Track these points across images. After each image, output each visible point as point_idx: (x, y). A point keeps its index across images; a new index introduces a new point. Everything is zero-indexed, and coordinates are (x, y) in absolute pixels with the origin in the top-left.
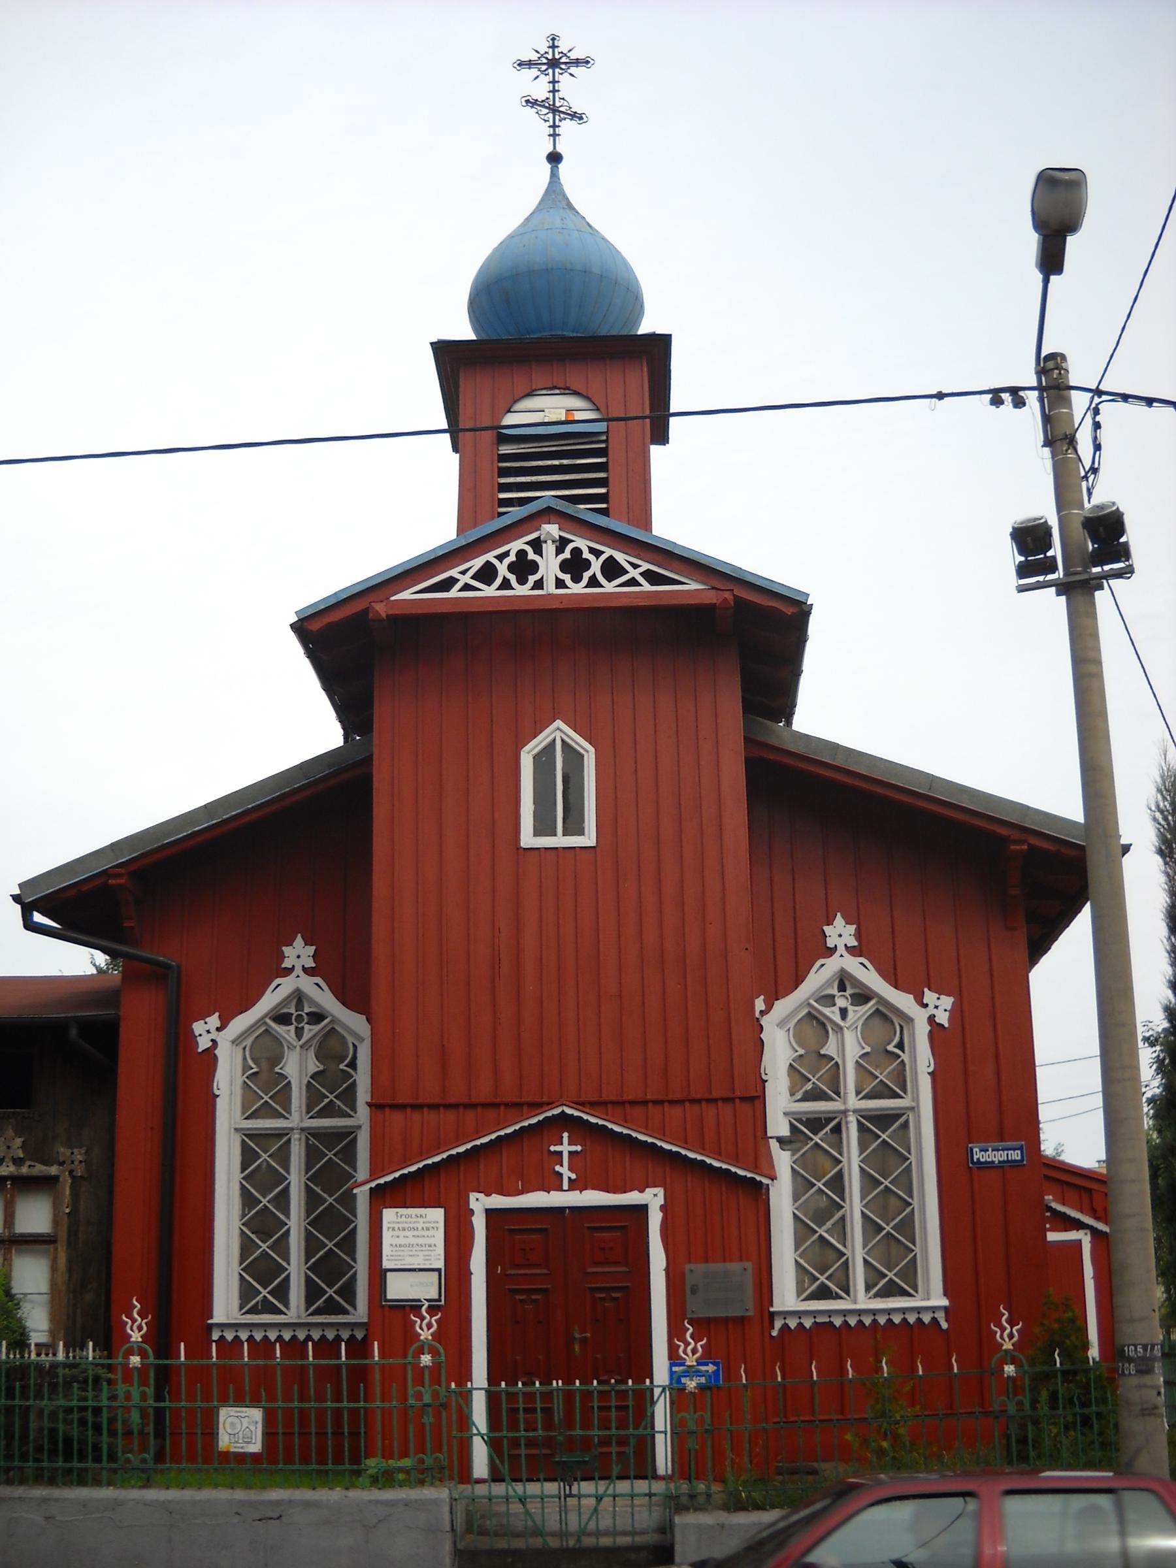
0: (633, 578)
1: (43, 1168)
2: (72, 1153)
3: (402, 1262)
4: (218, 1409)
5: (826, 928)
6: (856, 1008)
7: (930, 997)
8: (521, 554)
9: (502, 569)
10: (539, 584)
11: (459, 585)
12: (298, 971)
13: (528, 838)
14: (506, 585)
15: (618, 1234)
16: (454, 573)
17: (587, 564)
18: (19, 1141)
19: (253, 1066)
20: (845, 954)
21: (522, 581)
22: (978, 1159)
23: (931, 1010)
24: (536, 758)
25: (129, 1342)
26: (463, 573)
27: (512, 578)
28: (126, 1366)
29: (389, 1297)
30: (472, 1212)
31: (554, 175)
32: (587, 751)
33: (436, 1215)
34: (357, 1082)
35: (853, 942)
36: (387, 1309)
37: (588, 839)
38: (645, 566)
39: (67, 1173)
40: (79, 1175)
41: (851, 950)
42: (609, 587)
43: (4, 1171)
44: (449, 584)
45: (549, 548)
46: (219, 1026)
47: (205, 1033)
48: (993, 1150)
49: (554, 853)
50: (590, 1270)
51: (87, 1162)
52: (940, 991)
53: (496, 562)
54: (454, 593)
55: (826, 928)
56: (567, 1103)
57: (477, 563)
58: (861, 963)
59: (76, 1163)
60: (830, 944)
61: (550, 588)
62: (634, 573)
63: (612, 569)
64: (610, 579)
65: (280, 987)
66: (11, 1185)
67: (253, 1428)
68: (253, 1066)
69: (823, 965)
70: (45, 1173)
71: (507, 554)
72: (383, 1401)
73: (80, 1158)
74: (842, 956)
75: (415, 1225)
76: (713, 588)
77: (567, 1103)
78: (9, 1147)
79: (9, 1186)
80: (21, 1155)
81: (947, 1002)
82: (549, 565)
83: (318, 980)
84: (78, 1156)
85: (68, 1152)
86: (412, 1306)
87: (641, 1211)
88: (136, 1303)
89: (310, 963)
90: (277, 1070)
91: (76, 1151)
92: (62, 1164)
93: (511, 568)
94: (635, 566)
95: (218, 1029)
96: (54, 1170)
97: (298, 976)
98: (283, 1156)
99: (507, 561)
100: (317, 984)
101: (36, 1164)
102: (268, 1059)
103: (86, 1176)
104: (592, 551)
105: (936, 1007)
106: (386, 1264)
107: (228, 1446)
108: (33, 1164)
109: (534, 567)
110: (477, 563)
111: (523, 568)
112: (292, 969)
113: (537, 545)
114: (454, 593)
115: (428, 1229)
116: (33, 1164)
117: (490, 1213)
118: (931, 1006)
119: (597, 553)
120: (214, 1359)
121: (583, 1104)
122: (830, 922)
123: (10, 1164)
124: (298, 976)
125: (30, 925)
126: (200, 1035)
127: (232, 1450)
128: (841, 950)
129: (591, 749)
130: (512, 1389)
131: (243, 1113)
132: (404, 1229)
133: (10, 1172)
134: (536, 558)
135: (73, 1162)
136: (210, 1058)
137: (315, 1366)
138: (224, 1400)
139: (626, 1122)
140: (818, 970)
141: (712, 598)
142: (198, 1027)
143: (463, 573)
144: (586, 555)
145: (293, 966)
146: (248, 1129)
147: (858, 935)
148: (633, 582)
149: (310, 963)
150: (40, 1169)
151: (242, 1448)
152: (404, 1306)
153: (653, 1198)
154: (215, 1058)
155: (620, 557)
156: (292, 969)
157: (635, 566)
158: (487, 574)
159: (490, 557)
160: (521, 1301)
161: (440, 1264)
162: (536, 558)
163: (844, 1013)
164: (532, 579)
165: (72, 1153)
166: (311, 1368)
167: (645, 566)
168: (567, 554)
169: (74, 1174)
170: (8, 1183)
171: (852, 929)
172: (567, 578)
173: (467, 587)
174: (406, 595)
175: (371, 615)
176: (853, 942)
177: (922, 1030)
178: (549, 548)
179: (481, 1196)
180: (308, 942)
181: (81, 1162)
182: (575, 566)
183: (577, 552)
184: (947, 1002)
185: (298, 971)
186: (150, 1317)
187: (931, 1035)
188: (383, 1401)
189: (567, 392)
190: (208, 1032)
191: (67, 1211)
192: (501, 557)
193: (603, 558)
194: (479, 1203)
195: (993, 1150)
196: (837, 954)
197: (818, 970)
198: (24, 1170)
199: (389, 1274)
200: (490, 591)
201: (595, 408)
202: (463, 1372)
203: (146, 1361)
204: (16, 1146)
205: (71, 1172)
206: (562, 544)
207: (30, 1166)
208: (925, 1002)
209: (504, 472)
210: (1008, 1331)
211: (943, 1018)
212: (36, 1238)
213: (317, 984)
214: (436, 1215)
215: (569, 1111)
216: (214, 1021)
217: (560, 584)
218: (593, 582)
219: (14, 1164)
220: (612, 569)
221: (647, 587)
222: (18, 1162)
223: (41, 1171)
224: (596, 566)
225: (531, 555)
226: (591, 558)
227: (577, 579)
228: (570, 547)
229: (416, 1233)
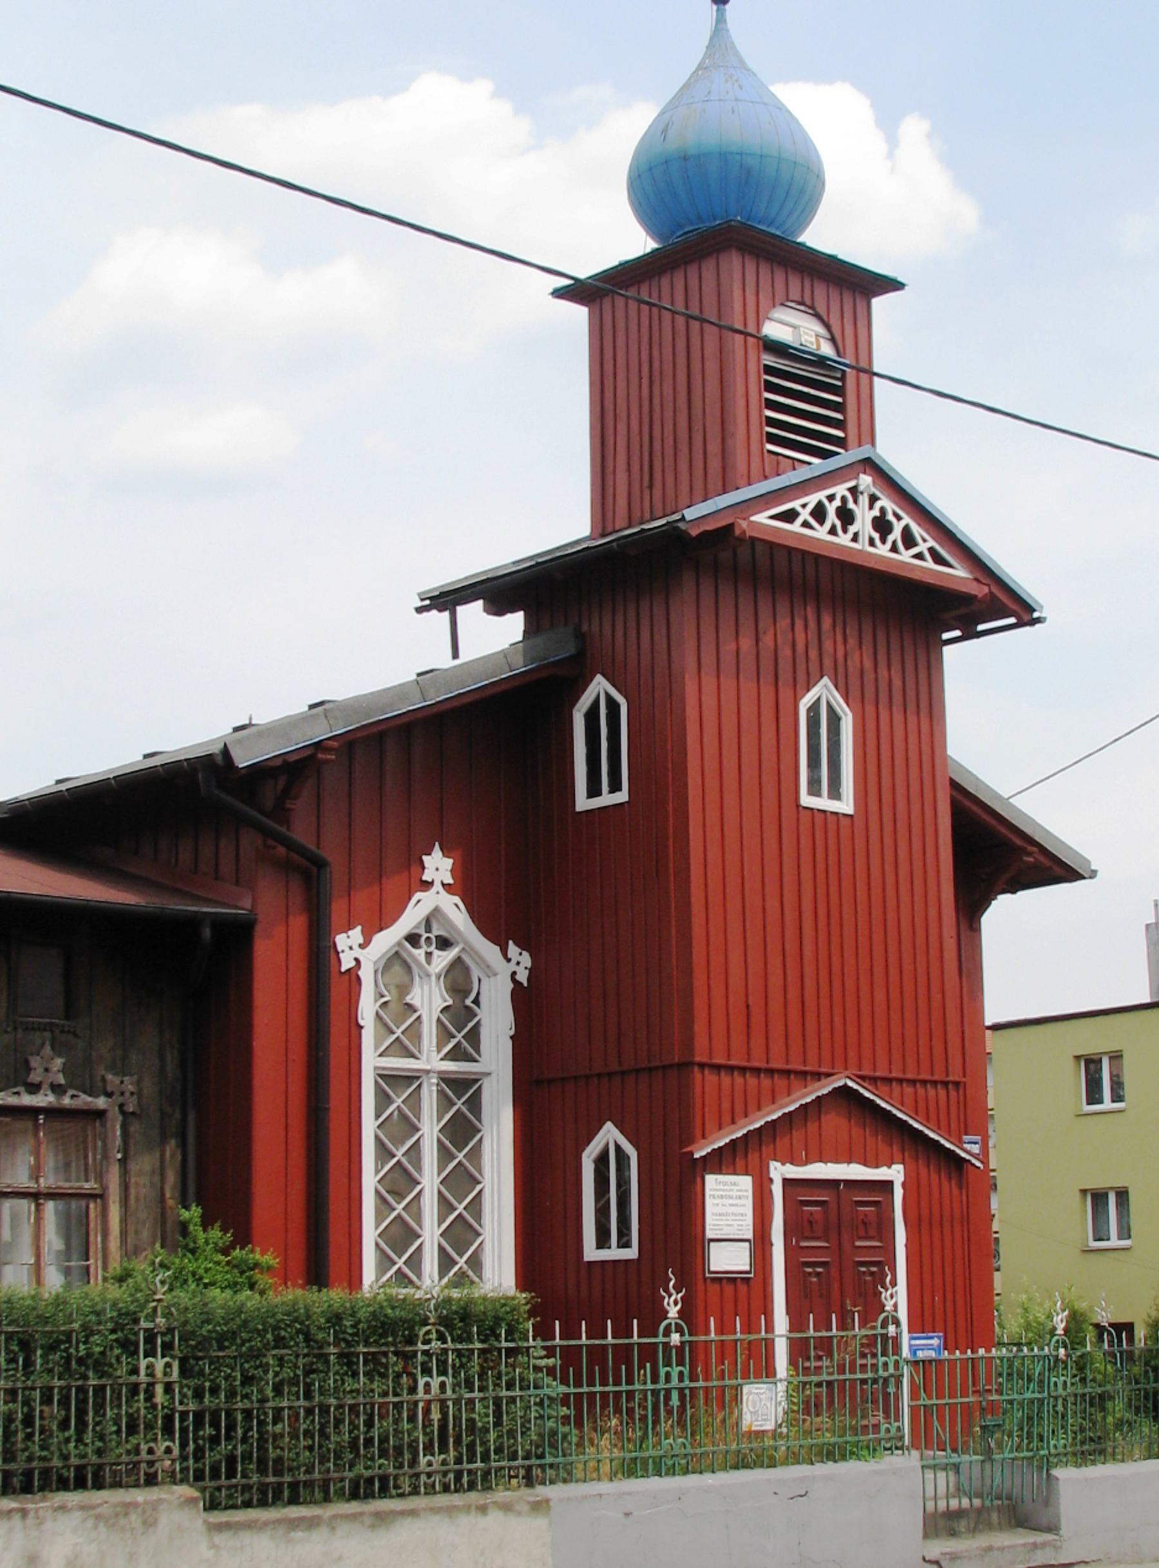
1: (90, 1099)
2: (122, 1082)
3: (722, 1232)
4: (741, 1385)
5: (425, 858)
6: (440, 953)
10: (855, 538)
12: (438, 886)
13: (806, 800)
15: (873, 1209)
16: (795, 504)
18: (59, 1062)
19: (386, 993)
24: (809, 710)
25: (884, 1311)
28: (666, 1345)
29: (712, 1269)
30: (771, 1180)
31: (721, 20)
32: (846, 715)
33: (745, 1183)
34: (483, 1022)
36: (725, 1281)
37: (846, 806)
38: (931, 543)
39: (117, 1108)
40: (131, 1110)
43: (42, 1101)
45: (864, 500)
46: (361, 941)
47: (347, 949)
49: (809, 812)
50: (858, 1243)
51: (139, 1094)
53: (826, 502)
54: (796, 527)
55: (425, 858)
56: (853, 1077)
57: (813, 499)
59: (127, 1094)
61: (862, 545)
65: (420, 903)
66: (44, 1119)
67: (769, 1405)
68: (386, 993)
70: (92, 1107)
72: (691, 1380)
73: (131, 1088)
75: (731, 1193)
76: (976, 579)
77: (853, 1077)
78: (47, 1070)
79: (41, 1121)
80: (63, 1081)
83: (457, 899)
84: (130, 1087)
85: (117, 1080)
86: (742, 1279)
87: (887, 1185)
88: (671, 1276)
89: (449, 880)
90: (408, 999)
91: (126, 1079)
92: (109, 1095)
94: (925, 540)
95: (362, 946)
96: (101, 1102)
97: (438, 893)
98: (415, 1101)
100: (456, 905)
101: (80, 1094)
102: (398, 987)
103: (138, 1112)
105: (351, 948)
106: (710, 1234)
107: (750, 1426)
108: (75, 1092)
110: (813, 499)
112: (431, 883)
114: (796, 527)
115: (740, 1198)
116: (75, 1092)
117: (786, 1182)
118: (514, 962)
119: (899, 518)
120: (713, 1335)
121: (863, 1078)
123: (49, 1092)
124: (438, 893)
126: (343, 951)
127: (754, 1428)
129: (850, 715)
130: (952, 1357)
131: (376, 1048)
132: (722, 1197)
133: (50, 1102)
135: (122, 1094)
136: (353, 978)
137: (614, 1346)
138: (746, 1375)
139: (891, 1098)
141: (980, 591)
142: (341, 941)
144: (890, 517)
146: (384, 1069)
149: (449, 880)
150: (85, 1100)
151: (761, 1426)
152: (735, 1279)
153: (895, 1173)
154: (359, 979)
155: (917, 530)
156: (431, 883)
157: (925, 540)
159: (821, 495)
160: (864, 1272)
161: (750, 1235)
163: (429, 955)
165: (122, 1082)
166: (610, 1347)
168: (876, 512)
169: (125, 1108)
170: (41, 1117)
174: (762, 518)
175: (737, 532)
178: (864, 500)
179: (778, 1164)
180: (446, 852)
181: (132, 1094)
182: (882, 525)
183: (883, 510)
185: (438, 886)
186: (684, 1290)
188: (691, 1380)
189: (810, 311)
190: (351, 948)
191: (119, 1156)
192: (831, 498)
194: (779, 1171)
198: (67, 1101)
199: (712, 1244)
201: (828, 336)
202: (501, 1358)
203: (684, 1339)
204: (55, 1069)
205: (121, 1106)
206: (873, 499)
207: (73, 1096)
209: (770, 387)
212: (78, 1191)
213: (456, 905)
214: (745, 1183)
215: (851, 1084)
216: (356, 934)
219: (53, 1092)
220: (909, 540)
221: (929, 564)
222: (58, 1089)
223: (86, 1103)
224: (896, 534)
225: (851, 505)
229: (731, 1201)
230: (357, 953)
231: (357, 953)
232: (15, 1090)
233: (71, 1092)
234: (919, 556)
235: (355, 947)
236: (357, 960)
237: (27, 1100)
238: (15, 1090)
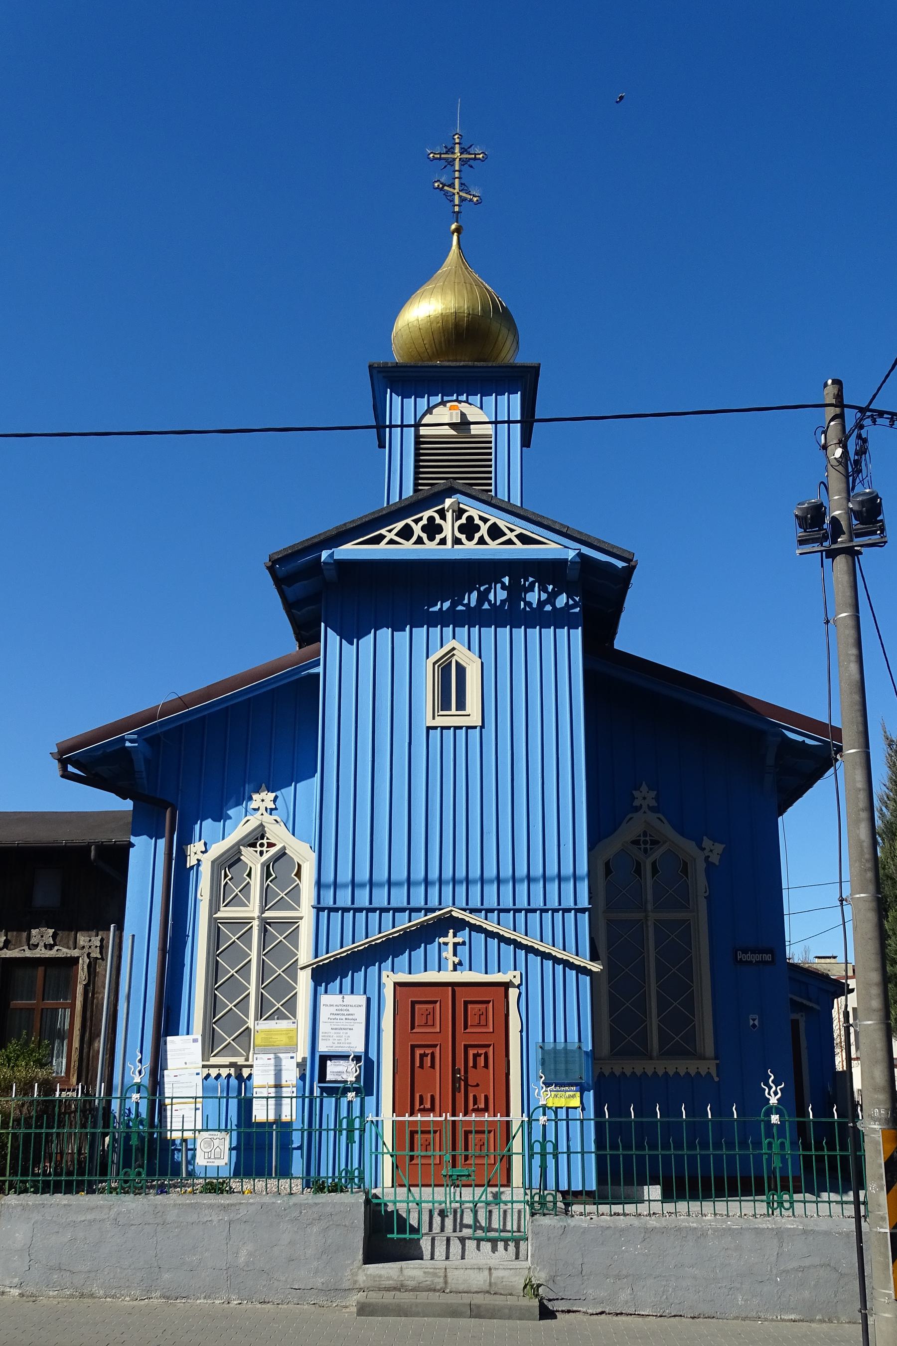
0: (510, 539)
7: (707, 843)
8: (431, 519)
9: (417, 530)
11: (386, 540)
14: (420, 541)
16: (383, 531)
17: (478, 529)
20: (647, 810)
21: (432, 538)
22: (741, 959)
23: (707, 853)
26: (390, 531)
27: (424, 536)
35: (653, 803)
41: (650, 808)
42: (493, 545)
44: (378, 539)
48: (751, 954)
52: (714, 840)
53: (413, 524)
57: (400, 525)
58: (659, 819)
60: (636, 803)
62: (510, 535)
63: (495, 532)
64: (494, 539)
69: (631, 818)
71: (421, 519)
74: (645, 812)
80: (52, 942)
81: (719, 848)
82: (449, 528)
93: (424, 529)
94: (512, 530)
99: (421, 524)
104: (481, 518)
109: (440, 529)
110: (400, 525)
111: (432, 529)
113: (442, 514)
119: (485, 520)
121: (465, 910)
122: (637, 788)
123: (43, 949)
125: (66, 775)
128: (645, 808)
134: (442, 522)
140: (628, 821)
143: (390, 531)
144: (477, 521)
145: (259, 807)
147: (657, 799)
148: (510, 542)
155: (502, 524)
157: (512, 530)
158: (406, 533)
159: (409, 521)
162: (442, 522)
164: (438, 537)
167: (519, 531)
168: (463, 520)
171: (653, 794)
172: (463, 537)
173: (392, 542)
176: (653, 803)
177: (701, 866)
178: (449, 515)
182: (470, 529)
183: (470, 519)
184: (719, 848)
187: (707, 871)
192: (416, 521)
193: (489, 524)
194: (389, 979)
195: (751, 954)
196: (642, 811)
197: (628, 821)
200: (408, 545)
206: (460, 513)
208: (703, 846)
210: (774, 1088)
211: (715, 859)
217: (457, 541)
218: (482, 541)
220: (495, 532)
225: (438, 520)
226: (481, 523)
227: (470, 538)
228: (465, 516)
230: (200, 856)
231: (200, 856)
232: (22, 948)
233: (56, 948)
234: (510, 542)
235: (198, 852)
236: (199, 860)
237: (28, 954)
238: (22, 948)
